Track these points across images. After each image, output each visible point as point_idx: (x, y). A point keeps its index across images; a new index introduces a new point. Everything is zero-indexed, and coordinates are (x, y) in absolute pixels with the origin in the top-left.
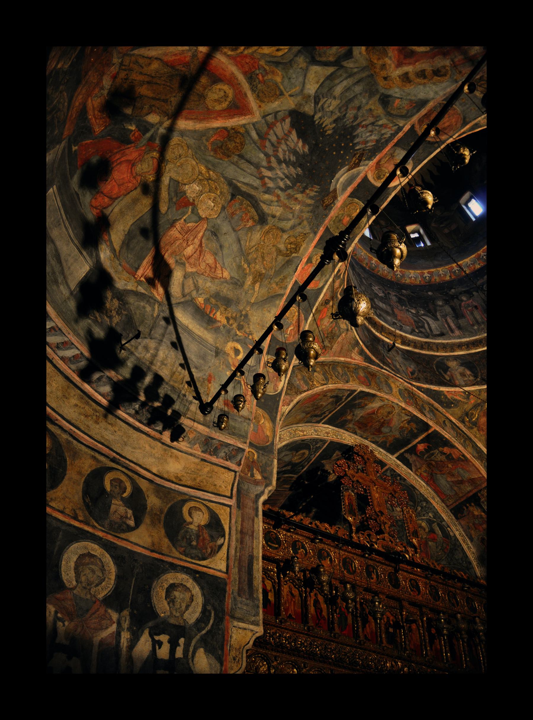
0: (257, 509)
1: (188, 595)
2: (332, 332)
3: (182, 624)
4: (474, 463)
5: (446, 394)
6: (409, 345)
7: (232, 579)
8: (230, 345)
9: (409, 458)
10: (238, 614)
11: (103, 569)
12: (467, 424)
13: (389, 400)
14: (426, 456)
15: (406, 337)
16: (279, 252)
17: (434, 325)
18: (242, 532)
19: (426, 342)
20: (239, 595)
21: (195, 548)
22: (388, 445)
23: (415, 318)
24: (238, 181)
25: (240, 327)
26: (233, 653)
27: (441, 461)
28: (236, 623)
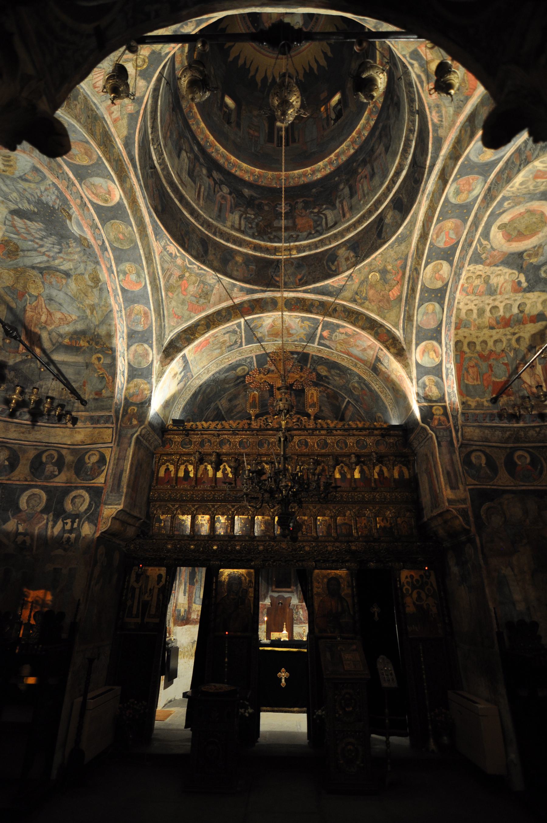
0: (130, 443)
1: (82, 499)
2: (203, 291)
3: (78, 512)
6: (304, 251)
7: (108, 484)
8: (94, 357)
10: (108, 502)
11: (40, 498)
15: (301, 245)
17: (330, 215)
18: (118, 459)
19: (320, 240)
20: (111, 492)
23: (316, 218)
24: (37, 263)
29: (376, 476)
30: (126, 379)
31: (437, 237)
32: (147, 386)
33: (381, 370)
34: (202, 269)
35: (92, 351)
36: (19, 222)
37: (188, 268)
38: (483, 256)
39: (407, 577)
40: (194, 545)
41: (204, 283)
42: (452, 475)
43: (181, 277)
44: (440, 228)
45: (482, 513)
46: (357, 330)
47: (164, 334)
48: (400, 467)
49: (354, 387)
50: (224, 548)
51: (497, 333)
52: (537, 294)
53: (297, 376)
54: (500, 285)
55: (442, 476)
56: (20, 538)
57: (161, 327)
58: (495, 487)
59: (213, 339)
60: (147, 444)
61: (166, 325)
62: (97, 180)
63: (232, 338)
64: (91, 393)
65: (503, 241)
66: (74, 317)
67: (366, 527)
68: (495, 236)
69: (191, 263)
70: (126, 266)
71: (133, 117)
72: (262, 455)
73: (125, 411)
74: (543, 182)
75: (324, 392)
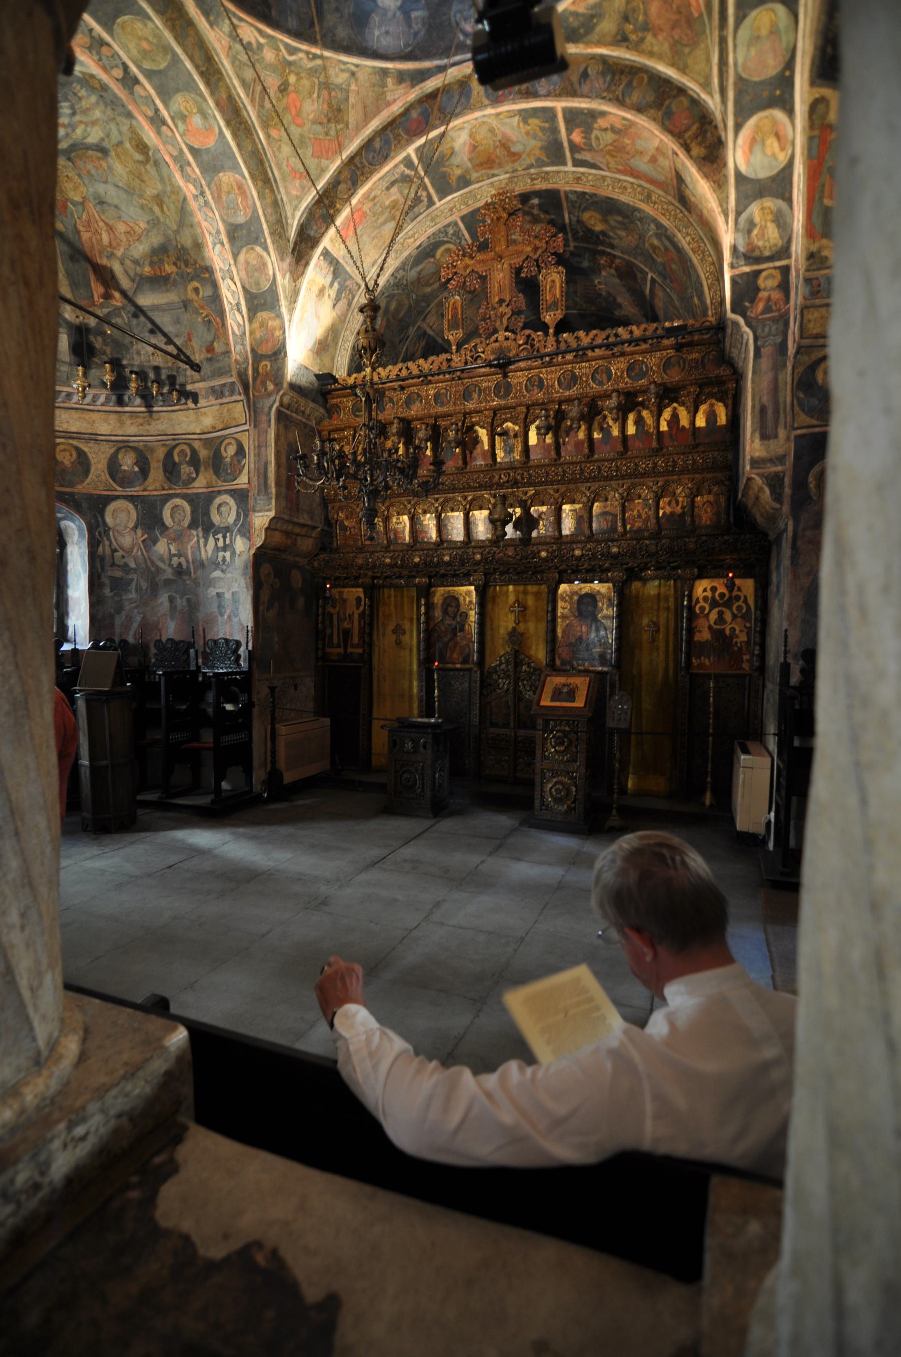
0: (270, 421)
2: (330, 105)
4: (641, 122)
5: (573, 9)
9: (584, 158)
11: (184, 511)
12: (633, 37)
13: (468, 122)
14: (594, 144)
18: (259, 446)
20: (258, 495)
21: (230, 474)
22: (546, 159)
25: (187, 263)
26: (257, 533)
27: (615, 141)
28: (256, 514)
29: (664, 427)
30: (246, 316)
32: (276, 323)
33: (690, 199)
34: (315, 57)
35: (186, 279)
37: (290, 64)
39: (705, 590)
40: (391, 558)
41: (326, 86)
42: (770, 411)
43: (284, 88)
45: (811, 479)
46: (628, 116)
47: (286, 218)
48: (712, 405)
49: (654, 248)
50: (429, 559)
53: (529, 249)
55: (749, 417)
56: (175, 561)
57: (276, 205)
59: (370, 205)
60: (300, 418)
61: (285, 199)
64: (201, 351)
66: (143, 225)
67: (640, 516)
69: (292, 51)
70: (180, 102)
72: (470, 413)
73: (256, 370)
75: (610, 267)
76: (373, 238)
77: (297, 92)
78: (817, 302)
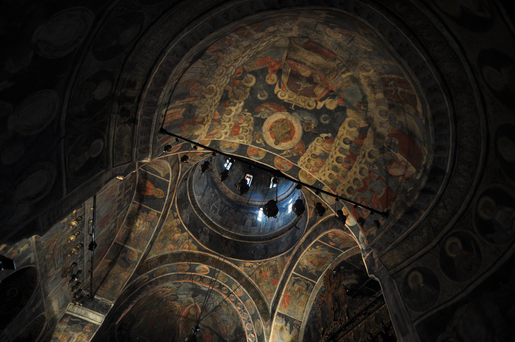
16: (227, 306)
31: (283, 168)
34: (266, 261)
36: (197, 298)
38: (295, 155)
41: (271, 266)
43: (261, 272)
44: (278, 166)
51: (356, 167)
52: (341, 129)
54: (323, 150)
58: (442, 307)
62: (197, 268)
63: (301, 284)
65: (290, 142)
68: (283, 147)
70: (234, 287)
71: (194, 242)
74: (243, 129)
76: (298, 303)
77: (264, 271)
78: (383, 252)
